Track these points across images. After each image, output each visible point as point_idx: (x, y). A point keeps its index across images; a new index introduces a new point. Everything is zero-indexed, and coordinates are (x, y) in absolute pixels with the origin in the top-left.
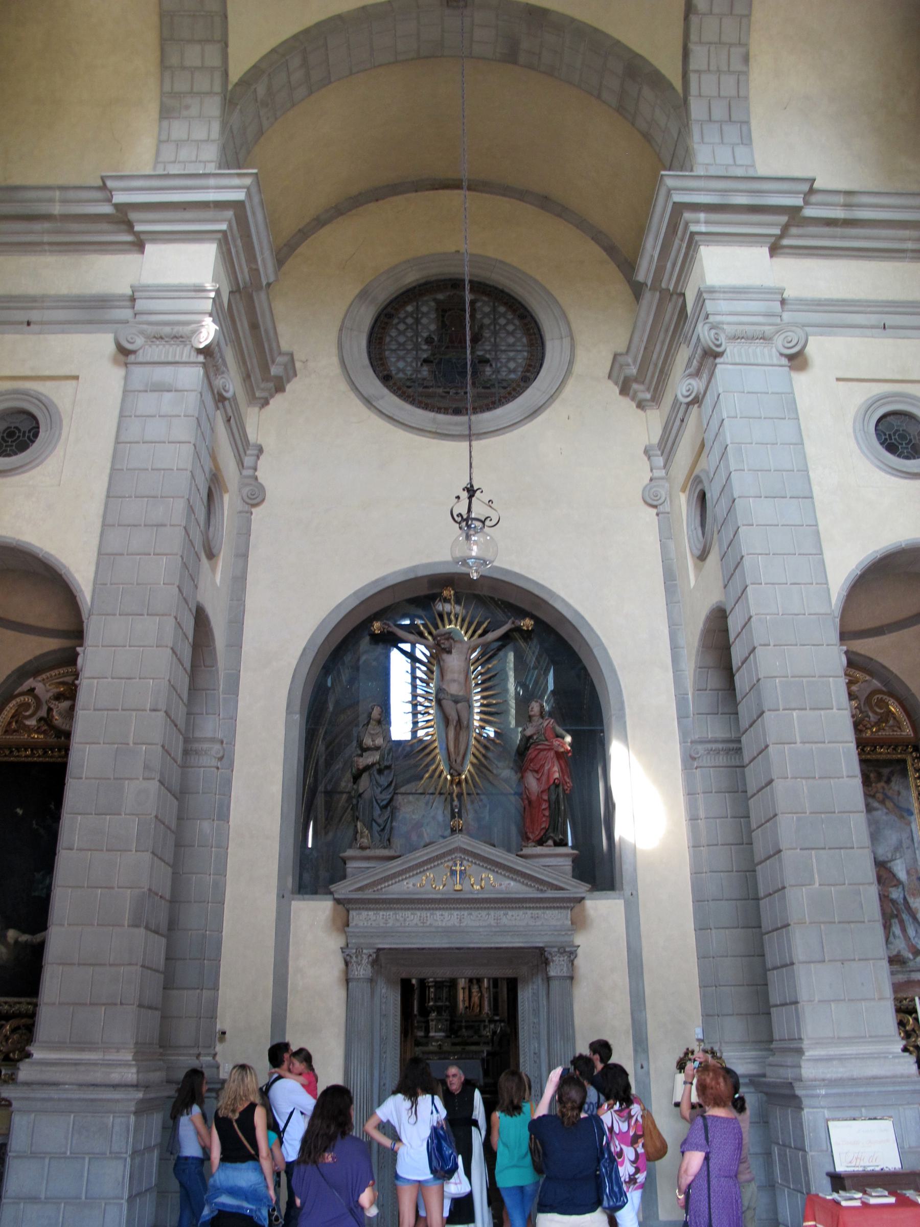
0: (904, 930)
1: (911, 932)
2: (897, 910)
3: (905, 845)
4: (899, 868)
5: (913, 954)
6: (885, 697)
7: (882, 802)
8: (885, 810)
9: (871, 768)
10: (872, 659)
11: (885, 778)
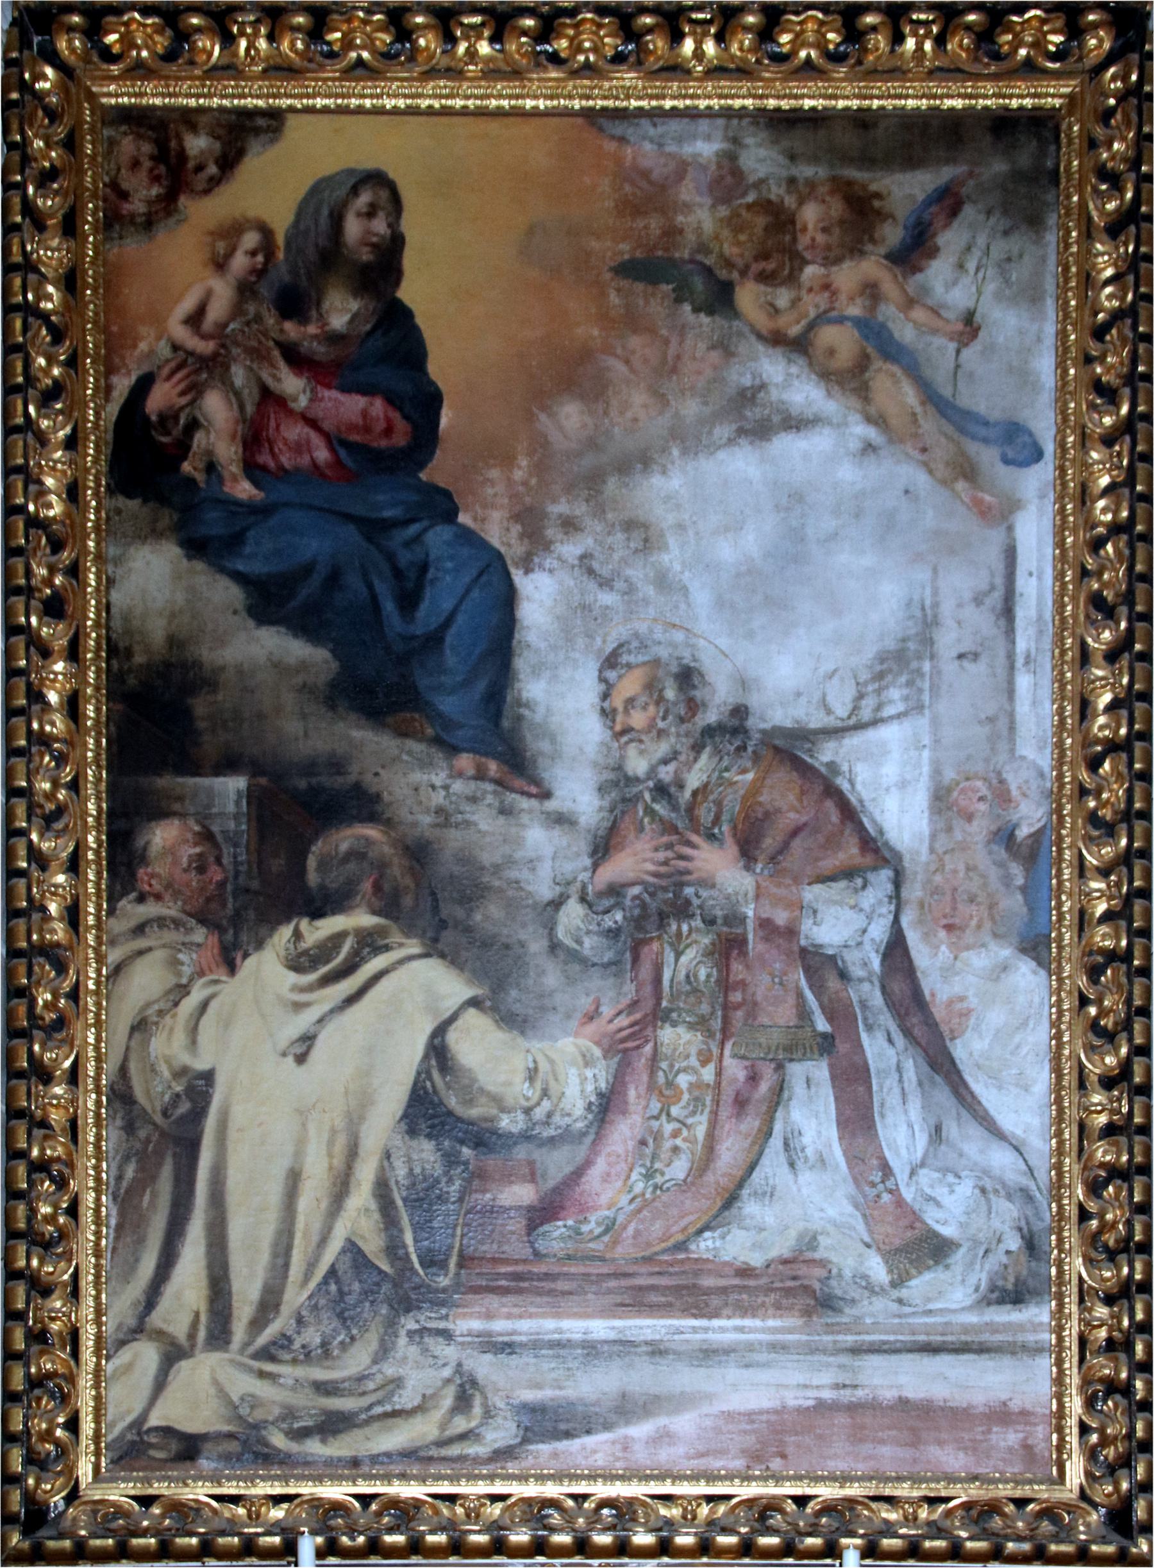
0: (857, 1119)
1: (901, 1132)
3: (948, 641)
5: (890, 1255)
7: (852, 380)
8: (860, 430)
9: (806, 171)
11: (893, 235)
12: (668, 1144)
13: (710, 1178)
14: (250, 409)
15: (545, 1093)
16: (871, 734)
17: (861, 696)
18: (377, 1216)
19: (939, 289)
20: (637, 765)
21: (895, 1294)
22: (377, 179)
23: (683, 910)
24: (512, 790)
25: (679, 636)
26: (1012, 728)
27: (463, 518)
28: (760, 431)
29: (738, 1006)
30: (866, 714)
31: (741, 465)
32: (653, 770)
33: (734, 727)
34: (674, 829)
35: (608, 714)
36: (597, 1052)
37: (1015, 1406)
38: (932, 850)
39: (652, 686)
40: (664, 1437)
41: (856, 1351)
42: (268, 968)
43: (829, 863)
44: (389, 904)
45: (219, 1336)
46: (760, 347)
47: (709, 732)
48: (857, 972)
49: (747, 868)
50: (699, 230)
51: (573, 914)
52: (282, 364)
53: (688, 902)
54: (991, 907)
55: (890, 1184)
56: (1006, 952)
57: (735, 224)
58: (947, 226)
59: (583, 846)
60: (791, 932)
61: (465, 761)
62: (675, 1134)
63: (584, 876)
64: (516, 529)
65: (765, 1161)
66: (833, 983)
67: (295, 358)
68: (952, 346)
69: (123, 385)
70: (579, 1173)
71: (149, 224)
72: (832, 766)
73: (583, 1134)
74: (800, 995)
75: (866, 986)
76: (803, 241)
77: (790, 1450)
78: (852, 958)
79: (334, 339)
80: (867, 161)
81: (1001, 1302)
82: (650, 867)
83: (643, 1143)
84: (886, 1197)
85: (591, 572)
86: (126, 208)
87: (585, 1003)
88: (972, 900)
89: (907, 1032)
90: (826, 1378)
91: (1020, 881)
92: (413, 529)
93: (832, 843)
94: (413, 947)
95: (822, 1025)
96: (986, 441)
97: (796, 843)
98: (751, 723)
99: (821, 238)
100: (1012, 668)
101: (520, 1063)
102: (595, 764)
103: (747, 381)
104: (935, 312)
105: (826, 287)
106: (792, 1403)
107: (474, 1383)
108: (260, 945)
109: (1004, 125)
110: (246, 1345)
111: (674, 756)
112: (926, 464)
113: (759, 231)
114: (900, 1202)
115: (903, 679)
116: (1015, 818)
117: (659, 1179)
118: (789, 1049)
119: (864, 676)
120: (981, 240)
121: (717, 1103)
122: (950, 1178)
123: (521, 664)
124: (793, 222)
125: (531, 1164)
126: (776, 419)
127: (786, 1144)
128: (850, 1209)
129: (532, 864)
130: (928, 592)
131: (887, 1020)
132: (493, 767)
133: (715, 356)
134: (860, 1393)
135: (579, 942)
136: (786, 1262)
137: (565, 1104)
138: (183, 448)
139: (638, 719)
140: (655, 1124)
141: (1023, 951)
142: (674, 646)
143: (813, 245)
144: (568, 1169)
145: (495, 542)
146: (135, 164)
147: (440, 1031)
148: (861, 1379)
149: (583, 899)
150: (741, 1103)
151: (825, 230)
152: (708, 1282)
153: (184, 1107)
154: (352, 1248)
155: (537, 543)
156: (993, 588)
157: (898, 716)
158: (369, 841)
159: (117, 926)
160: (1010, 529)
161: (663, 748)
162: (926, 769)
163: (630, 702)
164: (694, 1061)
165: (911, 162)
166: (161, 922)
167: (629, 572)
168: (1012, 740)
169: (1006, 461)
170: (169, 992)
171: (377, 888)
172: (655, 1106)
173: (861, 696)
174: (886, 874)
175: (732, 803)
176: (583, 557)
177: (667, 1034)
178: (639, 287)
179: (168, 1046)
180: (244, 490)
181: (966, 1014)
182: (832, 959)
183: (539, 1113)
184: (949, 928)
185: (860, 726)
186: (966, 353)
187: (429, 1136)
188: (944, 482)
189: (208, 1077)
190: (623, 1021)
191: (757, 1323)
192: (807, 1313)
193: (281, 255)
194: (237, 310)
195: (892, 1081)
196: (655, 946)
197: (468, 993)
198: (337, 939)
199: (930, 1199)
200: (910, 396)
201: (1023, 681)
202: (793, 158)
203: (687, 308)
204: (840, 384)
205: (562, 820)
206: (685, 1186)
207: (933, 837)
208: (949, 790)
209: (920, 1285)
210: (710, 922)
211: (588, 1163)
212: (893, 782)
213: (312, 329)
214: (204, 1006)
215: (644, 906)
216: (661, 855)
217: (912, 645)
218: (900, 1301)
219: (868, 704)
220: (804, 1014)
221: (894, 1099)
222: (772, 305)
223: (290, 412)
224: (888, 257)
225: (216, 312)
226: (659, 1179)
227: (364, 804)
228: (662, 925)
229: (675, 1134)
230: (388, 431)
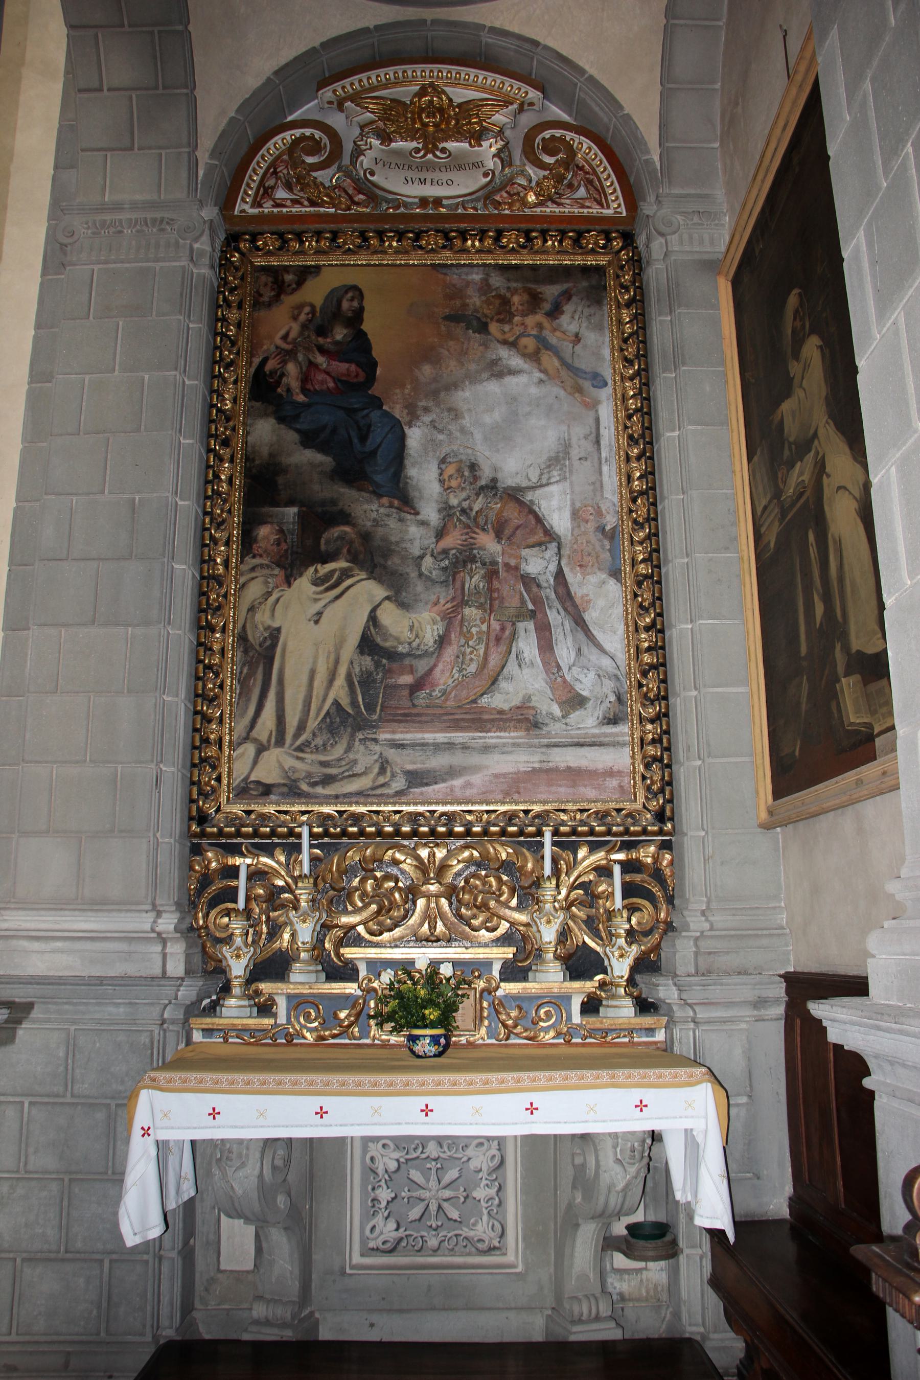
0: (546, 646)
1: (565, 652)
2: (538, 601)
3: (575, 453)
4: (555, 503)
5: (561, 704)
6: (569, 135)
7: (534, 357)
8: (538, 375)
9: (514, 285)
10: (536, 43)
11: (547, 306)
12: (468, 657)
13: (486, 671)
14: (304, 369)
15: (417, 636)
16: (546, 489)
17: (542, 474)
18: (347, 689)
19: (565, 325)
20: (454, 501)
21: (564, 721)
22: (355, 288)
23: (473, 559)
25: (470, 451)
26: (602, 486)
27: (384, 408)
28: (500, 375)
29: (496, 599)
30: (544, 481)
31: (493, 387)
32: (460, 504)
33: (492, 486)
34: (469, 527)
35: (442, 482)
36: (439, 618)
37: (615, 769)
38: (572, 535)
39: (459, 471)
40: (468, 785)
41: (548, 746)
42: (304, 584)
43: (532, 540)
44: (354, 558)
45: (280, 742)
47: (482, 488)
48: (544, 584)
49: (499, 542)
50: (474, 305)
51: (428, 561)
52: (317, 353)
53: (475, 556)
54: (597, 557)
57: (488, 302)
59: (432, 534)
60: (517, 568)
61: (385, 500)
62: (471, 653)
63: (433, 546)
64: (406, 411)
66: (535, 589)
67: (322, 350)
68: (571, 345)
69: (257, 361)
70: (431, 670)
71: (269, 305)
72: (531, 501)
73: (433, 653)
74: (521, 594)
75: (548, 590)
76: (513, 309)
77: (522, 790)
78: (542, 579)
79: (337, 343)
80: (537, 281)
81: (608, 723)
82: (459, 542)
83: (458, 657)
84: (559, 679)
85: (435, 427)
86: (262, 299)
87: (433, 598)
88: (589, 555)
89: (565, 610)
90: (536, 758)
91: (608, 547)
92: (366, 412)
93: (533, 532)
94: (363, 575)
95: (531, 606)
96: (585, 379)
97: (518, 532)
98: (498, 484)
99: (520, 308)
100: (600, 463)
101: (406, 623)
102: (437, 501)
103: (494, 357)
104: (564, 333)
105: (523, 324)
106: (522, 769)
107: (387, 762)
108: (301, 575)
109: (586, 270)
110: (292, 745)
111: (468, 498)
113: (497, 305)
114: (565, 681)
115: (558, 468)
117: (465, 672)
118: (517, 617)
119: (543, 466)
120: (580, 309)
122: (585, 671)
123: (407, 462)
125: (411, 666)
126: (505, 371)
127: (517, 657)
128: (544, 684)
129: (411, 541)
132: (396, 503)
133: (481, 348)
134: (550, 764)
135: (431, 573)
136: (518, 708)
137: (425, 640)
138: (278, 383)
139: (454, 483)
140: (463, 649)
141: (611, 575)
142: (467, 455)
143: (517, 310)
144: (427, 668)
145: (398, 417)
146: (266, 285)
147: (374, 610)
149: (432, 555)
150: (498, 640)
152: (486, 717)
153: (268, 643)
154: (336, 703)
155: (414, 417)
156: (591, 433)
158: (346, 533)
159: (244, 567)
160: (597, 411)
161: (464, 495)
163: (451, 477)
164: (478, 622)
166: (261, 566)
167: (450, 427)
168: (602, 492)
169: (594, 386)
170: (263, 595)
171: (349, 551)
172: (463, 641)
173: (542, 474)
174: (554, 544)
175: (492, 516)
176: (431, 422)
177: (467, 611)
178: (452, 324)
179: (263, 617)
180: (301, 398)
181: (589, 602)
183: (414, 644)
184: (580, 566)
185: (542, 486)
186: (576, 347)
187: (369, 655)
188: (570, 394)
189: (278, 630)
190: (449, 605)
191: (507, 734)
192: (527, 730)
193: (318, 314)
194: (301, 334)
195: (560, 630)
196: (462, 574)
197: (386, 594)
198: (333, 572)
199: (577, 680)
200: (556, 363)
201: (605, 469)
202: (508, 280)
203: (471, 331)
205: (424, 523)
206: (475, 675)
207: (573, 529)
208: (578, 511)
209: (574, 717)
210: (484, 564)
211: (435, 666)
212: (556, 508)
213: (329, 340)
214: (278, 600)
215: (457, 557)
216: (464, 537)
217: (561, 455)
218: (566, 724)
219: (545, 477)
220: (523, 602)
221: (561, 637)
223: (320, 370)
225: (293, 335)
226: (465, 672)
227: (344, 518)
228: (465, 566)
229: (471, 653)
230: (357, 376)
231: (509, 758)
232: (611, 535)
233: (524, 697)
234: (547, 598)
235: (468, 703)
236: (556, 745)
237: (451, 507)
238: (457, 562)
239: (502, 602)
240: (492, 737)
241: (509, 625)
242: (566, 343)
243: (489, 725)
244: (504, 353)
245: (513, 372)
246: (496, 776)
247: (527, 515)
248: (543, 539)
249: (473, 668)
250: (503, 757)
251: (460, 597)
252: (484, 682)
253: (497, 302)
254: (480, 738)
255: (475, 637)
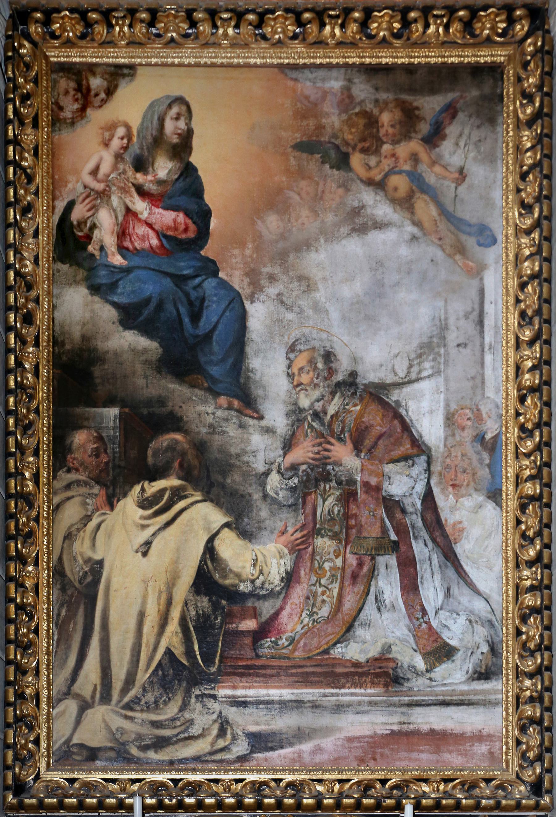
0: (410, 586)
3: (452, 337)
5: (426, 656)
7: (406, 203)
8: (410, 229)
9: (383, 96)
11: (424, 128)
12: (319, 599)
13: (340, 615)
16: (416, 386)
17: (411, 366)
19: (447, 156)
20: (305, 402)
21: (428, 675)
23: (326, 477)
24: (246, 415)
25: (324, 336)
26: (483, 383)
28: (362, 230)
30: (413, 376)
32: (312, 405)
33: (350, 384)
34: (322, 436)
36: (286, 551)
38: (445, 446)
39: (312, 362)
40: (318, 750)
41: (410, 705)
46: (362, 186)
47: (338, 385)
48: (410, 509)
49: (357, 455)
53: (329, 473)
54: (474, 474)
55: (426, 619)
56: (480, 498)
57: (349, 123)
58: (450, 123)
60: (378, 488)
62: (323, 593)
63: (279, 460)
65: (366, 607)
66: (399, 515)
68: (453, 185)
72: (397, 402)
74: (382, 521)
75: (414, 516)
76: (382, 132)
77: (378, 757)
78: (407, 502)
82: (311, 455)
84: (424, 626)
87: (280, 525)
88: (464, 471)
89: (434, 540)
90: (396, 719)
91: (487, 461)
93: (398, 443)
95: (393, 537)
96: (469, 234)
97: (381, 442)
99: (391, 130)
100: (483, 351)
102: (285, 402)
103: (356, 204)
104: (445, 167)
105: (393, 155)
106: (379, 732)
111: (322, 397)
112: (441, 246)
113: (361, 127)
114: (430, 627)
115: (431, 358)
116: (485, 429)
117: (315, 617)
119: (413, 356)
121: (343, 577)
122: (455, 615)
124: (377, 122)
126: (370, 223)
127: (376, 599)
128: (406, 632)
129: (254, 453)
130: (443, 312)
131: (424, 534)
133: (341, 191)
134: (411, 727)
135: (277, 494)
136: (376, 659)
139: (305, 378)
140: (314, 588)
141: (489, 497)
143: (387, 134)
148: (412, 720)
149: (279, 472)
150: (355, 577)
151: (392, 126)
152: (340, 670)
156: (473, 310)
157: (429, 377)
160: (482, 279)
161: (316, 394)
162: (442, 404)
163: (301, 369)
164: (332, 556)
165: (433, 91)
168: (483, 389)
169: (480, 245)
172: (314, 579)
173: (411, 366)
174: (424, 458)
175: (350, 420)
177: (319, 542)
181: (462, 530)
182: (398, 502)
184: (454, 486)
185: (411, 382)
186: (460, 189)
188: (449, 256)
190: (298, 535)
191: (363, 691)
192: (386, 685)
195: (426, 566)
196: (313, 496)
199: (445, 626)
200: (434, 211)
201: (488, 358)
202: (377, 89)
204: (400, 205)
205: (269, 431)
206: (328, 620)
207: (446, 439)
208: (453, 415)
209: (440, 671)
210: (339, 483)
212: (426, 411)
215: (308, 475)
216: (316, 449)
217: (435, 340)
218: (431, 679)
219: (415, 369)
220: (384, 531)
221: (428, 575)
222: (368, 165)
224: (422, 140)
226: (315, 617)
228: (317, 486)
229: (323, 593)
231: (365, 718)
232: (492, 446)
233: (383, 648)
234: (413, 527)
235: (318, 654)
236: (419, 704)
237: (301, 410)
238: (308, 480)
239: (360, 531)
240: (346, 695)
241: (367, 559)
242: (447, 183)
243: (343, 681)
244: (368, 196)
245: (379, 226)
246: (350, 739)
247: (391, 421)
248: (410, 451)
249: (325, 612)
250: (358, 717)
251: (311, 525)
252: (337, 629)
253: (362, 122)
254: (333, 695)
255: (328, 574)
